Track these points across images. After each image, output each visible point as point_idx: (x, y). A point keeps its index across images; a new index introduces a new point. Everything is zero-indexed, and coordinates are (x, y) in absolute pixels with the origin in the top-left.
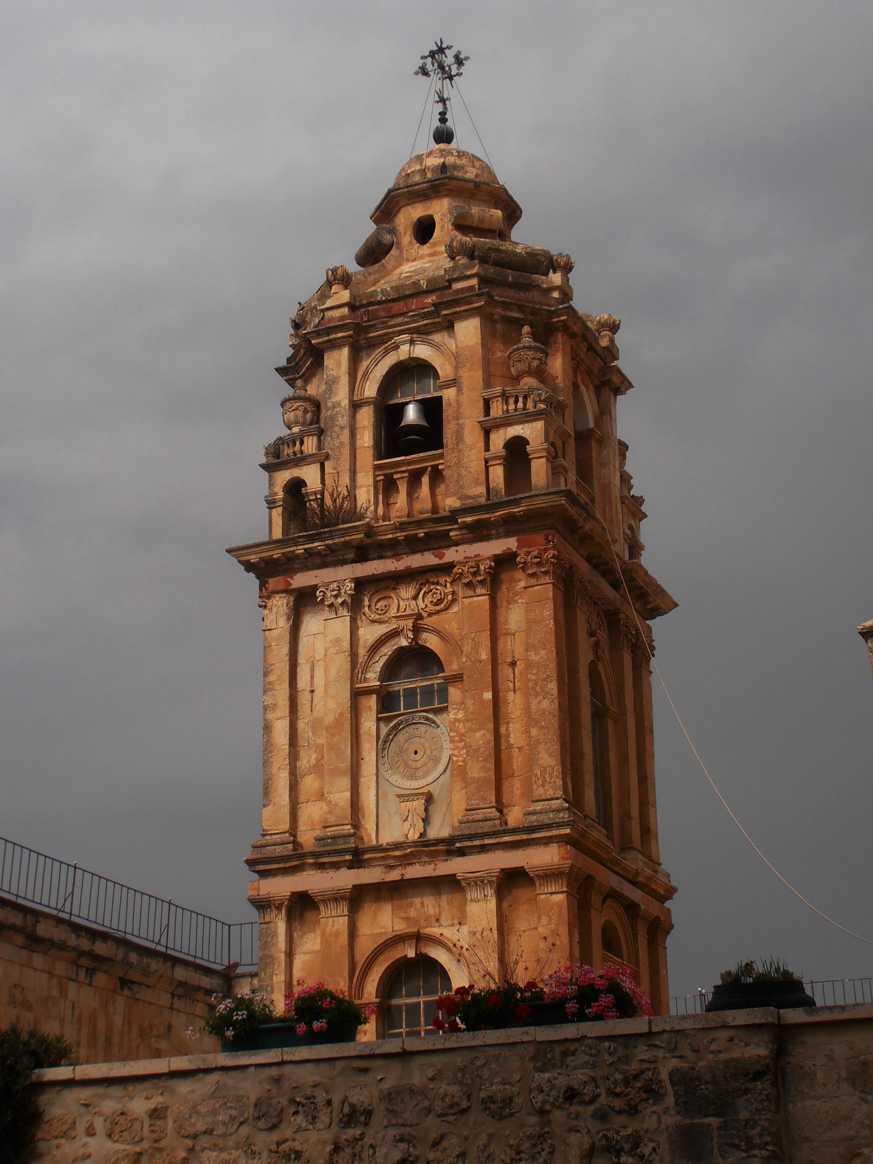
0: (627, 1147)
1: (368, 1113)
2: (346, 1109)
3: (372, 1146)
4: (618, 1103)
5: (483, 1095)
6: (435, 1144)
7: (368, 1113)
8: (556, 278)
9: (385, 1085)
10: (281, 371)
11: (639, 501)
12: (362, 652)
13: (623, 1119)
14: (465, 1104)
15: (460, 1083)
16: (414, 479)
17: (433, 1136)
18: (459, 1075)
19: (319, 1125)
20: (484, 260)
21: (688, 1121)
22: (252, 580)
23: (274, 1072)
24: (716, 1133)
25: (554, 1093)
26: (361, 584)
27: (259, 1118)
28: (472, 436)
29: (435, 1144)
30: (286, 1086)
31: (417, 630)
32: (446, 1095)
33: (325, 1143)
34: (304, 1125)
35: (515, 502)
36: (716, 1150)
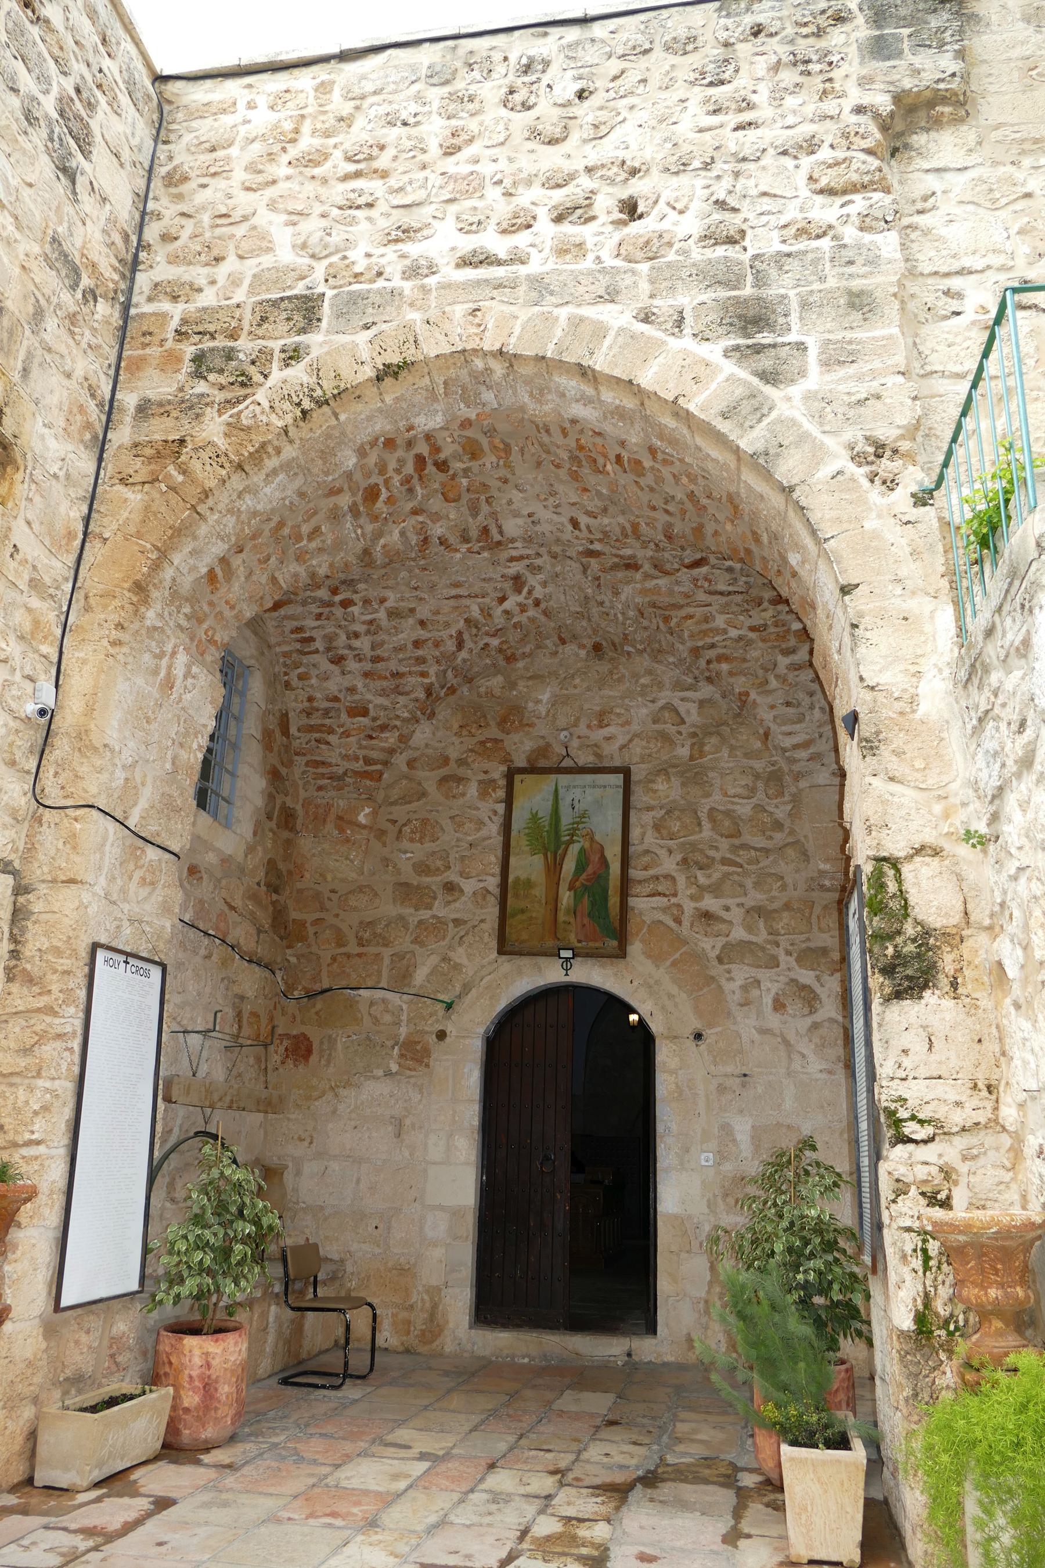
0: (815, 58)
2: (524, 61)
3: (549, 86)
4: (805, 31)
5: (667, 38)
6: (615, 78)
7: (546, 63)
9: (563, 42)
13: (811, 41)
14: (647, 46)
15: (643, 33)
17: (614, 71)
18: (642, 27)
19: (494, 75)
21: (878, 33)
23: (450, 43)
24: (906, 39)
25: (740, 29)
27: (431, 76)
29: (615, 78)
32: (628, 40)
33: (500, 87)
34: (479, 77)
36: (906, 51)
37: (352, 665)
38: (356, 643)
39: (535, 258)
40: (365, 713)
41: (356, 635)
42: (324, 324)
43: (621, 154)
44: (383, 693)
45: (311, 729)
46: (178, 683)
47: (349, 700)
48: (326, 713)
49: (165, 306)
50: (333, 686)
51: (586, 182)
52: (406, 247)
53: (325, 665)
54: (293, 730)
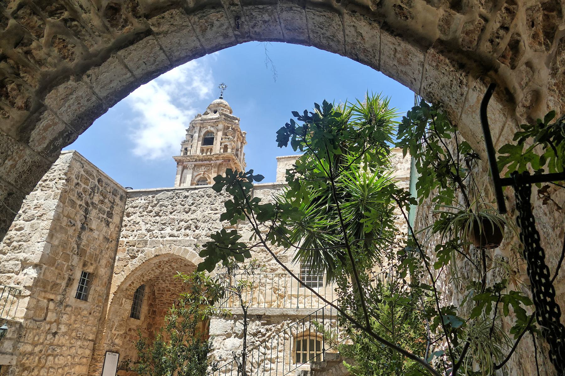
1: (188, 196)
7: (188, 196)
8: (237, 121)
10: (186, 130)
11: (246, 163)
12: (194, 177)
16: (208, 150)
20: (225, 116)
22: (176, 163)
26: (195, 165)
28: (219, 144)
30: (175, 192)
31: (204, 174)
35: (225, 154)
37: (167, 282)
38: (167, 278)
39: (181, 236)
40: (170, 291)
41: (167, 277)
42: (148, 246)
43: (196, 217)
44: (173, 287)
45: (159, 294)
46: (123, 304)
47: (167, 288)
48: (162, 291)
49: (124, 239)
50: (164, 286)
51: (190, 222)
52: (162, 232)
53: (161, 281)
54: (156, 294)
